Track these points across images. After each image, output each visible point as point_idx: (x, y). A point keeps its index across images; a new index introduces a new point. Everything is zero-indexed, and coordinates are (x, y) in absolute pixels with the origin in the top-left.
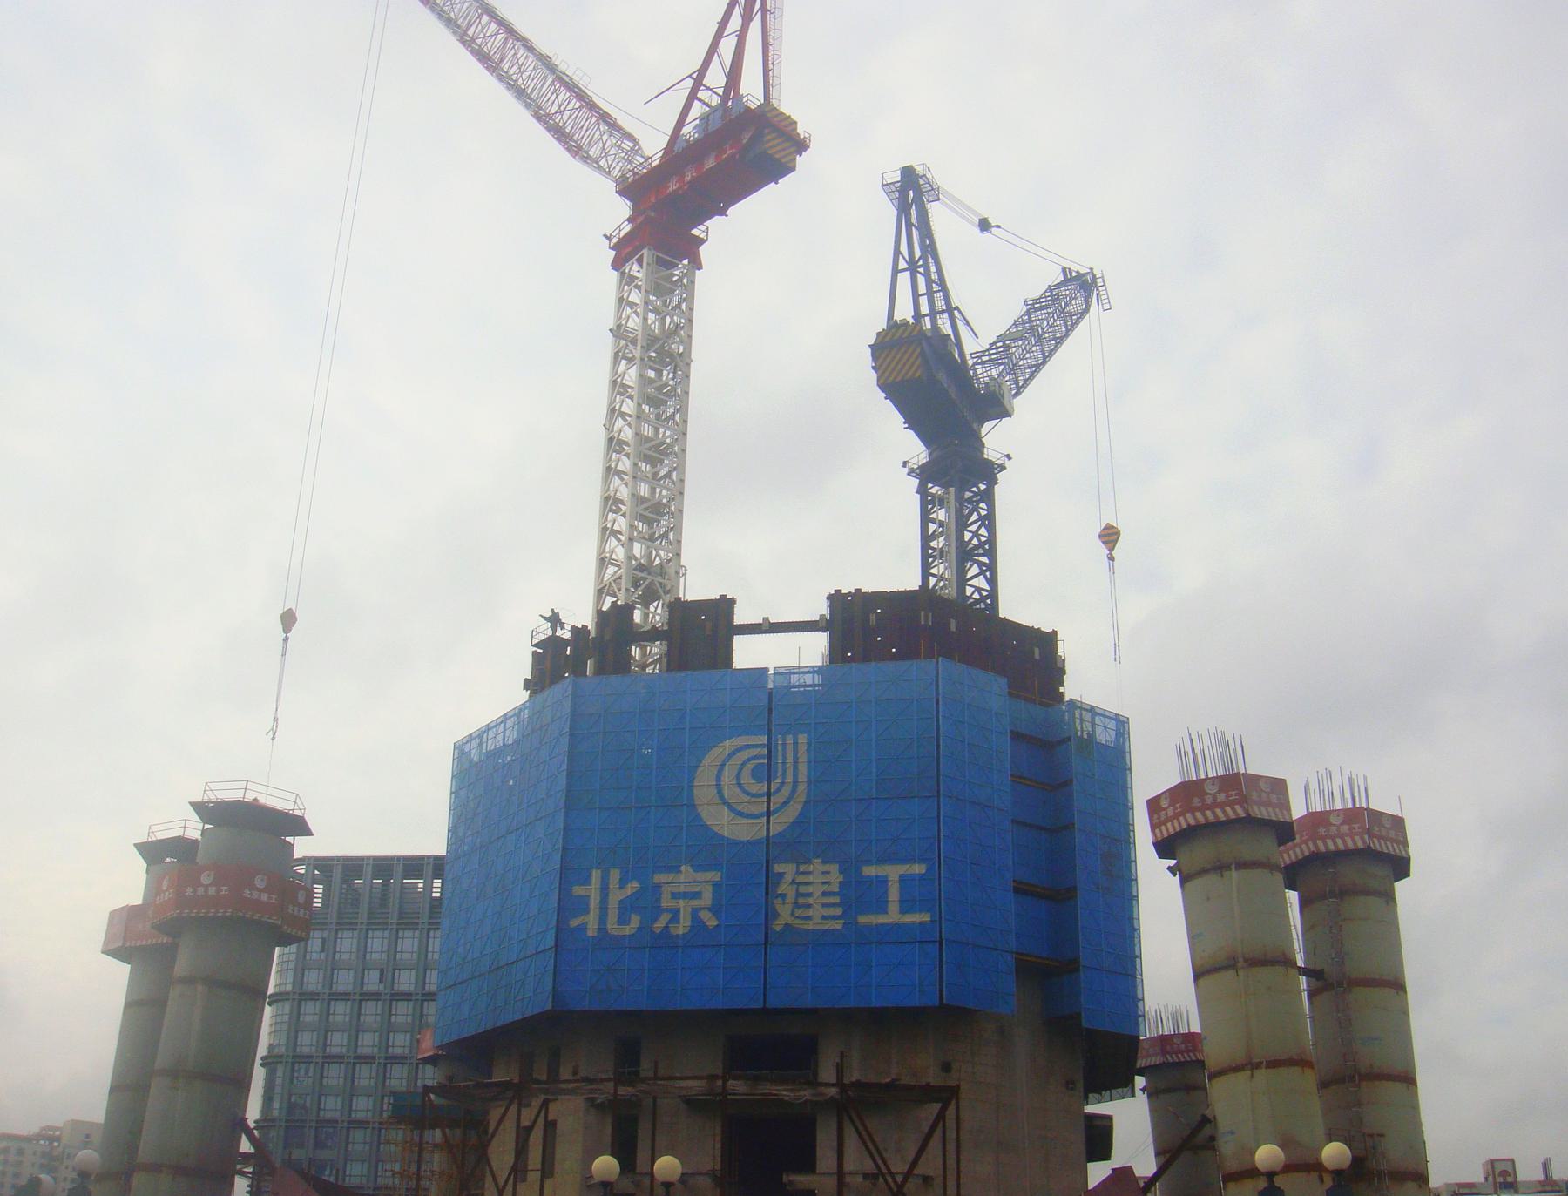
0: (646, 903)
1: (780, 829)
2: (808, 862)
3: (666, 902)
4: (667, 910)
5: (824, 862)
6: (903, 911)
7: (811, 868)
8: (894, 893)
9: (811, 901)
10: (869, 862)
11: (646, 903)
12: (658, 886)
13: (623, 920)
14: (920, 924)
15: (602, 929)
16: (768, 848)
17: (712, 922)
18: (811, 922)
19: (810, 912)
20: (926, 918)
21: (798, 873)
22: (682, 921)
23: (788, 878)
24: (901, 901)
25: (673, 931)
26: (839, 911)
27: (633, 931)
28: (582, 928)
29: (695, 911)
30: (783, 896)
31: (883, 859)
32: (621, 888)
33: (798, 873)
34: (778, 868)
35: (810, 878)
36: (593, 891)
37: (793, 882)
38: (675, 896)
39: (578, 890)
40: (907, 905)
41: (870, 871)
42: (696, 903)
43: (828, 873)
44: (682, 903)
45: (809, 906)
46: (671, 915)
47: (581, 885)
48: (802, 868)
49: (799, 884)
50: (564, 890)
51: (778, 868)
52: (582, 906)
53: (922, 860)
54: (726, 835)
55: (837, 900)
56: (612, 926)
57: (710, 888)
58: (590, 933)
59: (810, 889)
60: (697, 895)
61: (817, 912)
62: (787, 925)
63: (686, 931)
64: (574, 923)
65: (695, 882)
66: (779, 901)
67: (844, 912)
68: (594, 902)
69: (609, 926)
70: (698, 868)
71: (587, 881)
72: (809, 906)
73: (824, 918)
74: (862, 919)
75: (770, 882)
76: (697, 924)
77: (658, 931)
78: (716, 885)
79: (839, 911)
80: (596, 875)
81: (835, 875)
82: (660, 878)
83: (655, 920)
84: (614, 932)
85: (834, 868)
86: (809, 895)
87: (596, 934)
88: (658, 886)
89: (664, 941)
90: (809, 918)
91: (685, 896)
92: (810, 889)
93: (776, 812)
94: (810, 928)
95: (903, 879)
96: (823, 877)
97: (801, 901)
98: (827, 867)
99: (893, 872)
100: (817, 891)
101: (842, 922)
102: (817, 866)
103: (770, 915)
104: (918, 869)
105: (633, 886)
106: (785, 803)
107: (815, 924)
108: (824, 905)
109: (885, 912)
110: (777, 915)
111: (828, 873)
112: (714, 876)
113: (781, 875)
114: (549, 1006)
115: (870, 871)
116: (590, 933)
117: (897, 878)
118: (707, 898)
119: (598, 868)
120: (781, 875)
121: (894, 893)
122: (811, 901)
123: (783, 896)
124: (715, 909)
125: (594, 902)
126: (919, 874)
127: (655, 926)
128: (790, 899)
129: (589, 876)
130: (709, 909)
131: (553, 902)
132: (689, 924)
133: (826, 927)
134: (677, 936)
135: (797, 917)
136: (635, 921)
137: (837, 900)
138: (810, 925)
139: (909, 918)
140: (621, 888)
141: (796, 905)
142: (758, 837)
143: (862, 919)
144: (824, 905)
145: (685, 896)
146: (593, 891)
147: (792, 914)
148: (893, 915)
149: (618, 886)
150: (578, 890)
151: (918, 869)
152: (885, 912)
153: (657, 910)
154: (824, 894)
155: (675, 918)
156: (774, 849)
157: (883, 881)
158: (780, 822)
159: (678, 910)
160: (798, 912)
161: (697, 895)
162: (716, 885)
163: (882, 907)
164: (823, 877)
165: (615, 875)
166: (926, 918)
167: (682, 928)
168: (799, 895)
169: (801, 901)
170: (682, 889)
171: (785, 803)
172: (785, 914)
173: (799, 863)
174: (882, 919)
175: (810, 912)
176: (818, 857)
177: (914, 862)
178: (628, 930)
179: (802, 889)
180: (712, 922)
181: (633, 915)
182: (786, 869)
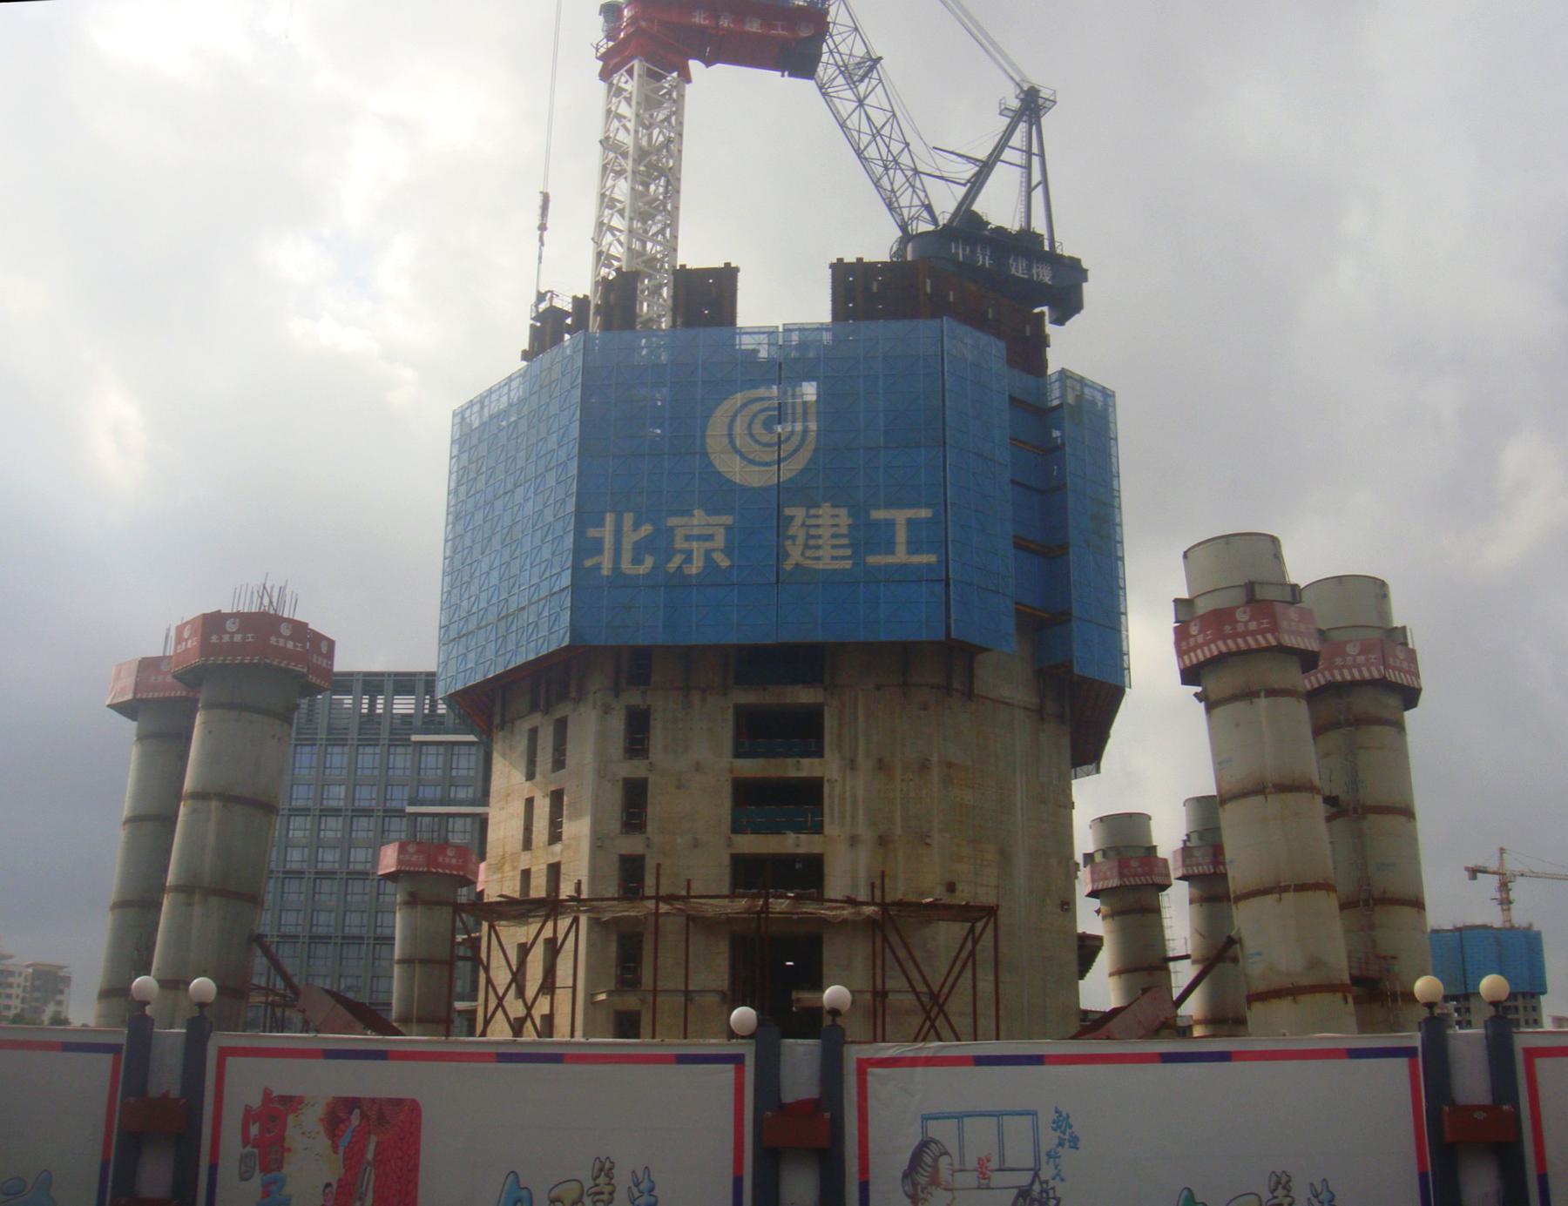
0: (660, 544)
1: (789, 475)
2: (819, 506)
3: (679, 544)
4: (681, 551)
5: (833, 506)
6: (910, 552)
7: (821, 512)
8: (901, 536)
9: (821, 542)
10: (878, 507)
11: (660, 544)
12: (672, 529)
13: (637, 560)
14: (926, 564)
15: (616, 567)
16: (779, 492)
17: (723, 561)
18: (821, 562)
19: (820, 553)
20: (932, 559)
21: (808, 516)
22: (695, 562)
23: (798, 521)
24: (909, 543)
25: (687, 571)
26: (848, 552)
27: (647, 571)
28: (598, 567)
29: (708, 553)
30: (794, 538)
31: (889, 505)
32: (634, 530)
33: (808, 516)
34: (788, 511)
35: (820, 521)
36: (607, 533)
37: (803, 525)
38: (688, 538)
39: (592, 533)
40: (914, 546)
41: (879, 514)
42: (709, 545)
43: (837, 516)
44: (695, 545)
45: (818, 547)
46: (683, 556)
47: (597, 526)
48: (812, 512)
49: (809, 526)
50: (579, 532)
51: (788, 511)
52: (597, 547)
53: (928, 506)
54: (738, 481)
55: (845, 541)
56: (626, 566)
57: (722, 530)
58: (605, 572)
59: (820, 531)
60: (710, 538)
61: (826, 552)
62: (797, 565)
63: (700, 570)
64: (588, 563)
65: (708, 525)
66: (788, 543)
67: (853, 553)
68: (608, 543)
69: (623, 566)
70: (709, 512)
71: (601, 523)
72: (818, 547)
73: (833, 558)
74: (871, 560)
75: (782, 523)
76: (709, 562)
77: (671, 571)
78: (728, 528)
79: (848, 552)
80: (609, 519)
81: (844, 518)
82: (673, 521)
83: (669, 560)
84: (628, 572)
85: (843, 512)
86: (819, 537)
87: (610, 573)
88: (672, 529)
89: (679, 582)
90: (818, 558)
91: (700, 538)
92: (820, 531)
93: (786, 459)
94: (821, 567)
95: (910, 523)
96: (832, 520)
97: (812, 542)
98: (836, 511)
99: (901, 516)
100: (826, 532)
101: (851, 562)
102: (826, 510)
103: (782, 555)
104: (924, 513)
105: (646, 529)
106: (796, 451)
108: (834, 547)
109: (893, 553)
110: (787, 555)
111: (837, 516)
112: (727, 519)
113: (792, 518)
114: (566, 642)
115: (879, 514)
116: (605, 572)
117: (903, 522)
118: (720, 541)
119: (610, 512)
120: (792, 518)
121: (901, 536)
122: (821, 542)
123: (794, 538)
124: (728, 551)
125: (608, 543)
126: (926, 518)
127: (669, 566)
128: (801, 540)
129: (603, 519)
130: (722, 550)
131: (569, 542)
132: (701, 564)
133: (836, 567)
134: (690, 576)
135: (808, 558)
136: (649, 562)
137: (845, 541)
138: (820, 566)
139: (919, 559)
140: (634, 530)
141: (806, 547)
142: (770, 483)
143: (871, 560)
144: (834, 547)
145: (700, 538)
146: (607, 533)
147: (803, 554)
148: (901, 556)
149: (631, 528)
150: (592, 533)
151: (924, 513)
152: (893, 553)
153: (670, 552)
154: (834, 536)
155: (688, 556)
156: (784, 493)
157: (890, 524)
158: (790, 469)
159: (692, 551)
160: (809, 553)
161: (710, 538)
162: (728, 528)
163: (890, 548)
164: (832, 520)
165: (629, 518)
166: (932, 559)
167: (695, 568)
168: (809, 537)
169: (812, 542)
170: (695, 531)
171: (796, 451)
172: (795, 555)
173: (809, 507)
174: (890, 559)
175: (820, 553)
176: (826, 502)
177: (921, 507)
178: (642, 570)
179: (813, 531)
180: (723, 561)
181: (647, 556)
182: (798, 513)
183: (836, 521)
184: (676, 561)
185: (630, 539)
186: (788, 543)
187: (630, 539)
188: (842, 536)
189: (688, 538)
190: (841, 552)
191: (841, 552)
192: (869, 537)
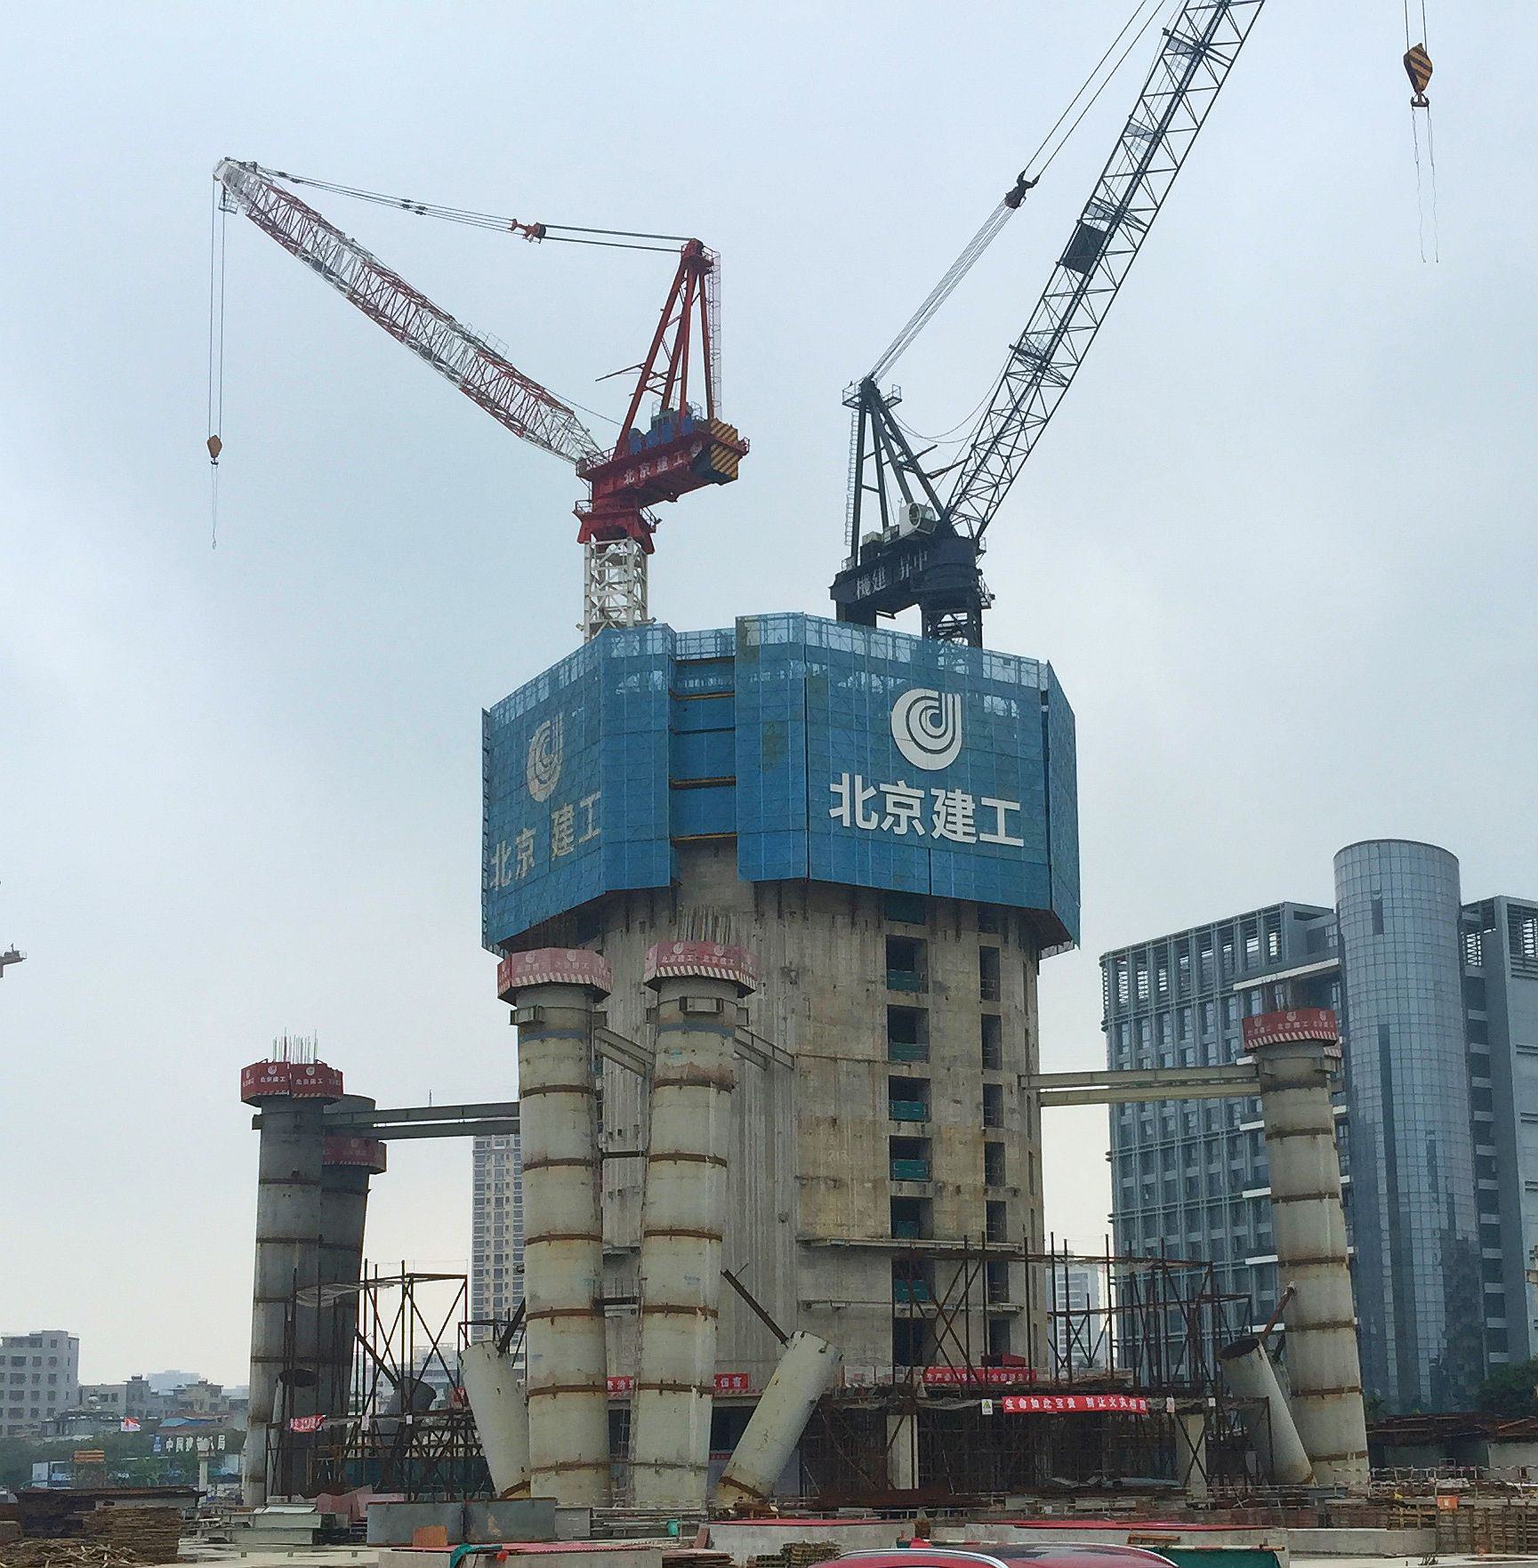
0: (877, 805)
3: (890, 809)
13: (867, 818)
33: (947, 798)
36: (844, 789)
38: (896, 804)
41: (986, 801)
48: (950, 795)
49: (947, 806)
56: (861, 823)
60: (910, 807)
73: (965, 834)
80: (846, 777)
90: (955, 832)
100: (960, 812)
105: (871, 792)
107: (959, 838)
128: (943, 815)
141: (947, 822)
147: (945, 826)
153: (883, 815)
160: (948, 825)
161: (910, 807)
164: (963, 802)
165: (858, 780)
168: (948, 814)
169: (950, 818)
179: (951, 810)
183: (964, 805)
184: (890, 820)
185: (861, 796)
186: (935, 817)
187: (861, 796)
188: (968, 817)
189: (896, 804)
190: (968, 830)
191: (968, 830)
192: (984, 818)
